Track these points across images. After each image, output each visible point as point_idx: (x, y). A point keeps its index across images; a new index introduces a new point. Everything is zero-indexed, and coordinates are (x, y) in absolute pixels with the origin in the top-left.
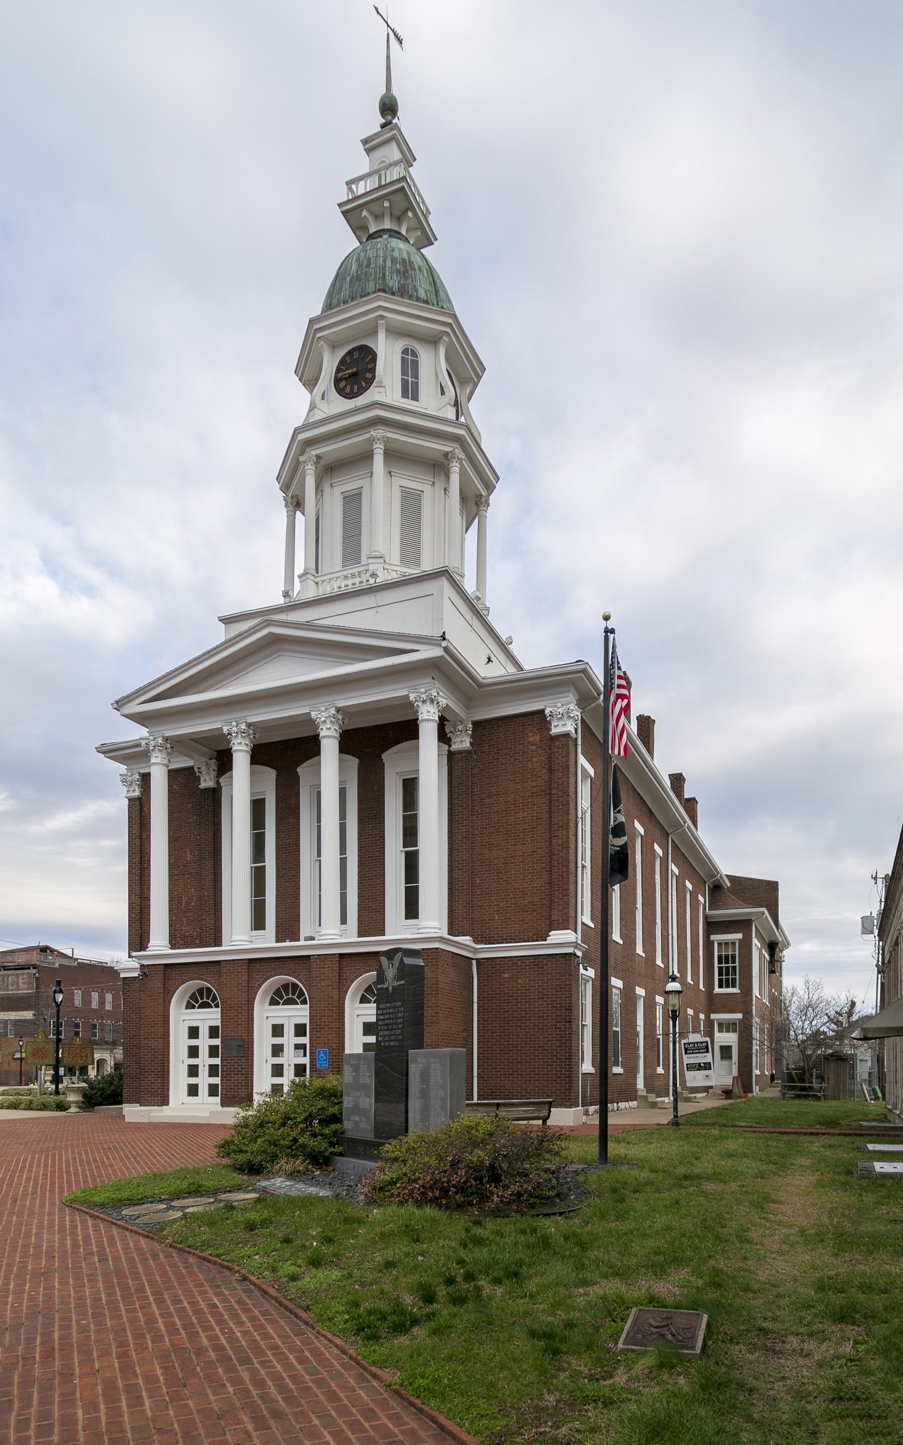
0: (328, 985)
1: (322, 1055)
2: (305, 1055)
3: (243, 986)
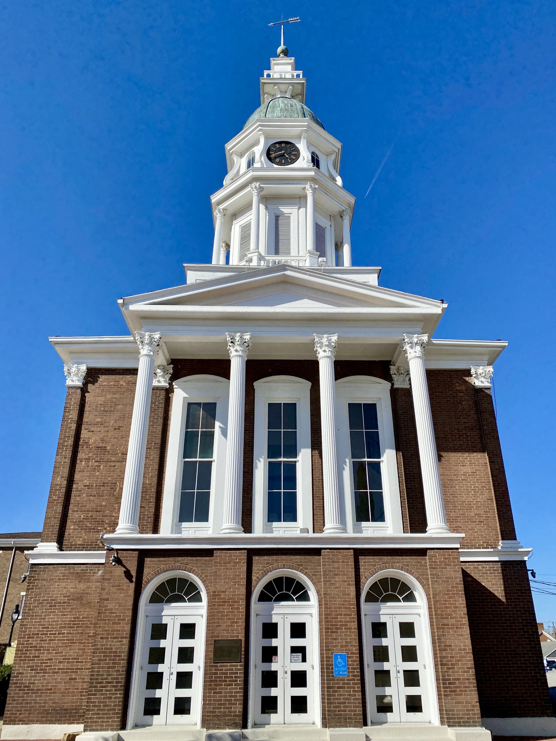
0: (344, 581)
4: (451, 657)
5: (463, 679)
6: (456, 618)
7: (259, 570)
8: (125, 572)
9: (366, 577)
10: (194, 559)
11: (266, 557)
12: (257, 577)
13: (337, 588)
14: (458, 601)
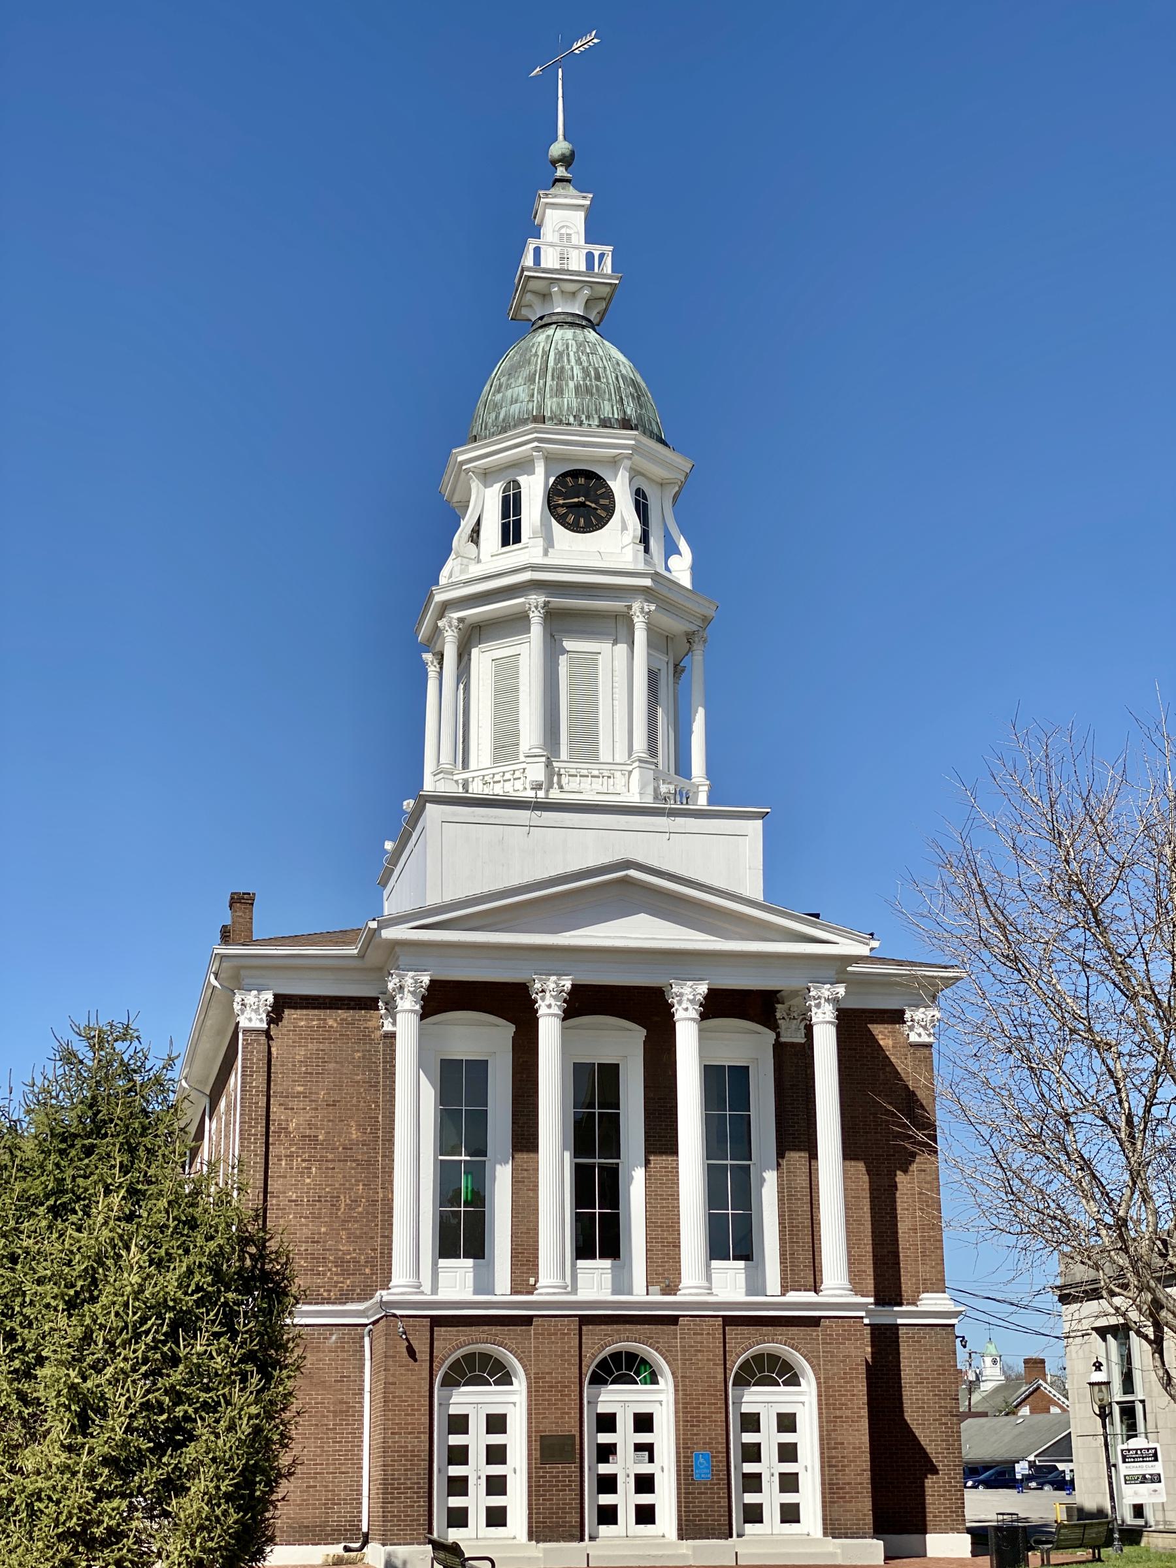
0: (708, 1360)
1: (701, 1460)
2: (651, 1460)
3: (572, 1356)
4: (842, 1457)
5: (856, 1484)
6: (853, 1408)
7: (595, 1344)
8: (407, 1347)
9: (737, 1354)
10: (506, 1328)
11: (603, 1327)
12: (592, 1354)
13: (700, 1369)
14: (857, 1387)
